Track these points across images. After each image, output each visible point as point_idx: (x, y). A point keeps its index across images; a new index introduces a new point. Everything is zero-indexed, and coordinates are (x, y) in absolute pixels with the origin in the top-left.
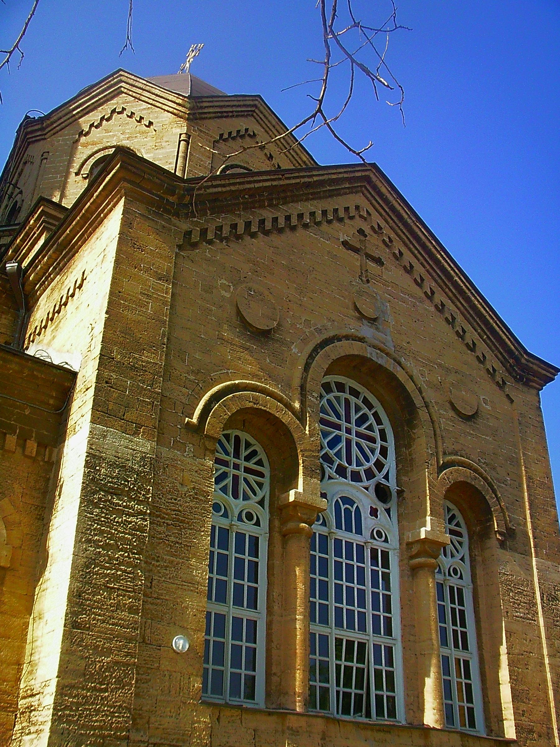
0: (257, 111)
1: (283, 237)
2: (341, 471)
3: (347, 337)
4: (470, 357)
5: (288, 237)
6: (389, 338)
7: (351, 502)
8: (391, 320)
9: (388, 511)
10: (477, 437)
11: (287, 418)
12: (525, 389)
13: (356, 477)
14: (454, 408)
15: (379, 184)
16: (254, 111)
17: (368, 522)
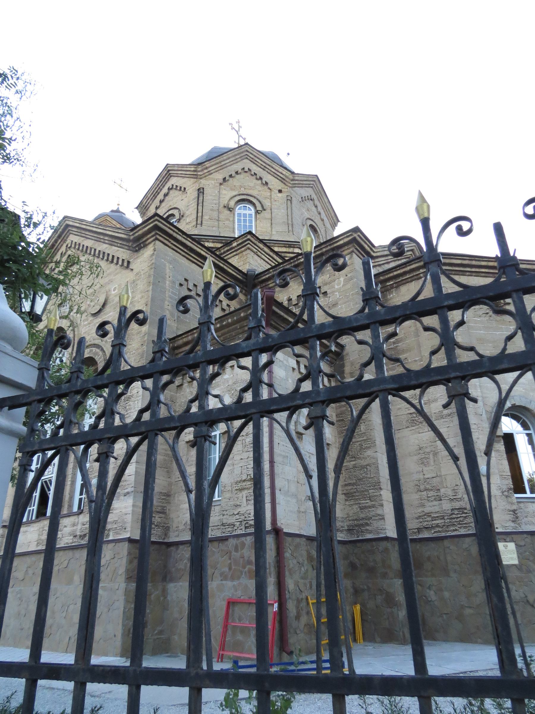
0: (170, 172)
16: (170, 174)
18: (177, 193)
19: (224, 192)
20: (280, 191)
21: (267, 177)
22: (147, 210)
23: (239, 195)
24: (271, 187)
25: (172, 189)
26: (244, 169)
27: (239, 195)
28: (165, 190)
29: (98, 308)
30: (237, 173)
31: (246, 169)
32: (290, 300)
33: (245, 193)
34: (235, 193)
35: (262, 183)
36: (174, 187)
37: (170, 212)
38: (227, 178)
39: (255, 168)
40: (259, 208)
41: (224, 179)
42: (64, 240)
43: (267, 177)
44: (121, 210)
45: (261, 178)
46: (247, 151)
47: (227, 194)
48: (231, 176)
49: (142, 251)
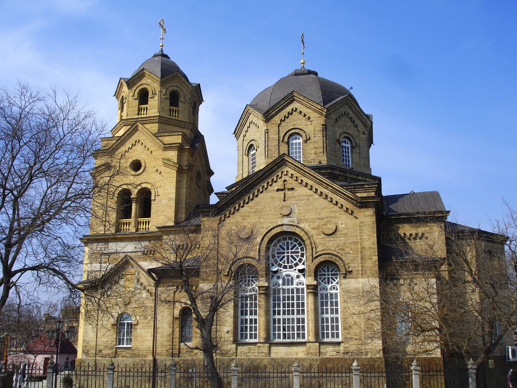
1: (253, 201)
2: (285, 267)
3: (277, 227)
4: (336, 208)
5: (256, 199)
6: (295, 218)
7: (289, 276)
8: (296, 211)
9: (304, 275)
10: (335, 240)
11: (254, 263)
12: (366, 209)
13: (291, 267)
14: (324, 234)
15: (288, 159)
17: (296, 281)
18: (301, 116)
19: (336, 129)
20: (364, 133)
21: (358, 122)
22: (272, 118)
23: (344, 133)
24: (359, 129)
25: (295, 111)
26: (345, 112)
27: (344, 133)
28: (289, 109)
29: (331, 232)
30: (342, 115)
31: (347, 113)
32: (405, 234)
33: (346, 131)
34: (341, 131)
35: (354, 125)
36: (298, 110)
37: (297, 131)
38: (338, 119)
39: (351, 114)
40: (354, 145)
41: (336, 119)
42: (278, 168)
43: (358, 122)
44: (165, 52)
45: (354, 122)
46: (348, 100)
47: (339, 131)
48: (339, 117)
49: (363, 210)
